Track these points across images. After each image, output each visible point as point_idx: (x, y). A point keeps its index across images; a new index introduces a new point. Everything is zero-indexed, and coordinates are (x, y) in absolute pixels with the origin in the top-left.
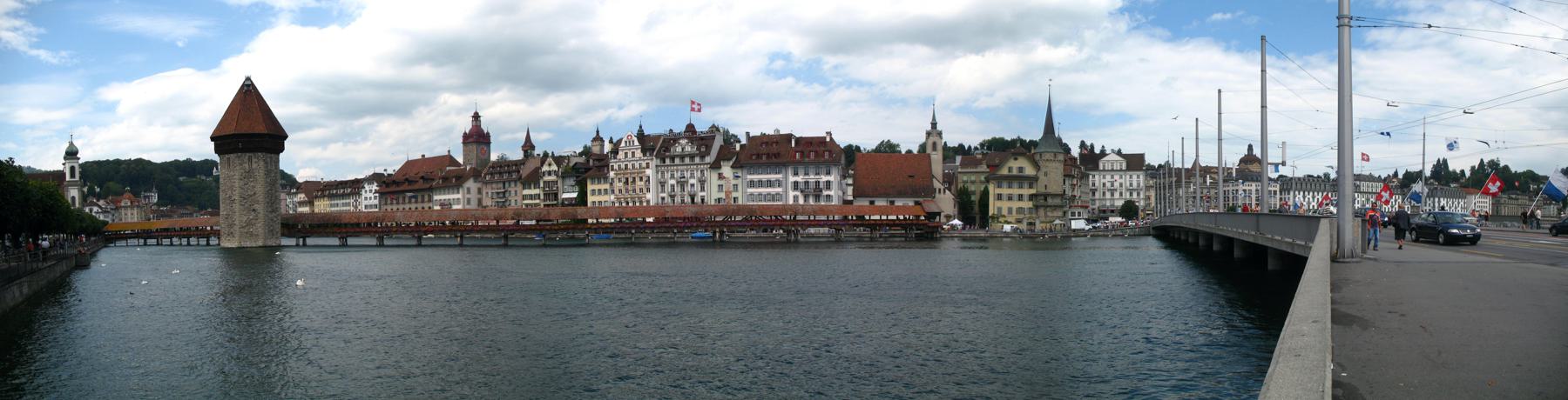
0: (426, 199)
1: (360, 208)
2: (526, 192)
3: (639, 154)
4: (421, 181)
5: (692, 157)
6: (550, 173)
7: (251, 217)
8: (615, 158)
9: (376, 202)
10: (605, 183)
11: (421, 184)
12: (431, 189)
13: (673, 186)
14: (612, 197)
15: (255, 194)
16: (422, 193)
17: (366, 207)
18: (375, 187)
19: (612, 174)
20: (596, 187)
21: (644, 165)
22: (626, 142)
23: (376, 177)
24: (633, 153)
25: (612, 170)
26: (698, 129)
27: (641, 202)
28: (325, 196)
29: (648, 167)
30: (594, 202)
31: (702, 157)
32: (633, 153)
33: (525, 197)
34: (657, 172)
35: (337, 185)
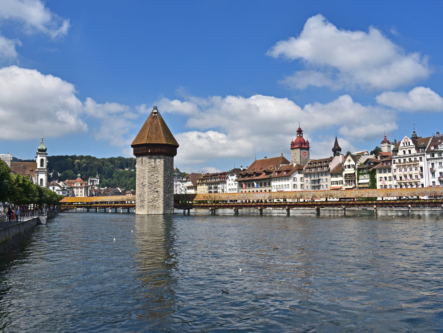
0: (267, 183)
1: (225, 190)
2: (334, 179)
3: (414, 151)
6: (349, 167)
8: (396, 155)
11: (263, 176)
12: (270, 179)
15: (158, 181)
16: (265, 181)
18: (235, 177)
19: (394, 166)
20: (383, 175)
21: (418, 158)
22: (404, 143)
24: (410, 151)
25: (394, 163)
27: (417, 185)
28: (203, 183)
29: (421, 160)
32: (410, 151)
33: (332, 183)
34: (428, 164)
35: (211, 176)
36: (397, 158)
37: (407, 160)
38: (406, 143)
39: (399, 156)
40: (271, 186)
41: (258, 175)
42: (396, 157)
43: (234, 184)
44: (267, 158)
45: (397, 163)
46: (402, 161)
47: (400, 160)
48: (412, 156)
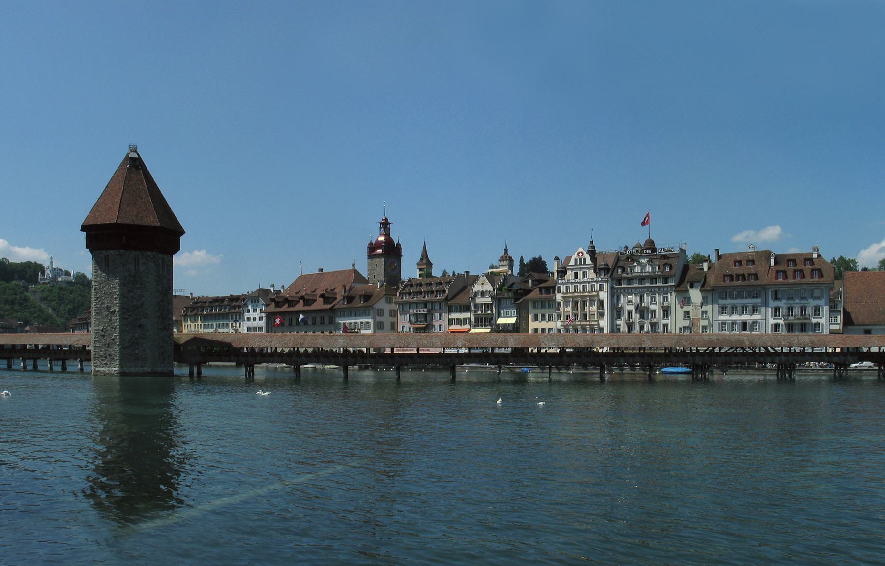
4: (321, 299)
5: (653, 279)
7: (136, 335)
9: (262, 323)
10: (549, 307)
11: (319, 304)
13: (630, 312)
14: (559, 324)
15: (142, 304)
17: (249, 329)
21: (597, 287)
22: (576, 260)
23: (263, 293)
24: (584, 274)
25: (558, 292)
26: (658, 246)
30: (536, 330)
31: (666, 280)
32: (584, 274)
35: (211, 302)
36: (563, 284)
37: (580, 287)
38: (580, 260)
39: (568, 280)
40: (334, 322)
41: (307, 302)
42: (563, 281)
43: (257, 319)
44: (323, 272)
45: (563, 293)
46: (572, 289)
47: (567, 288)
48: (589, 282)
